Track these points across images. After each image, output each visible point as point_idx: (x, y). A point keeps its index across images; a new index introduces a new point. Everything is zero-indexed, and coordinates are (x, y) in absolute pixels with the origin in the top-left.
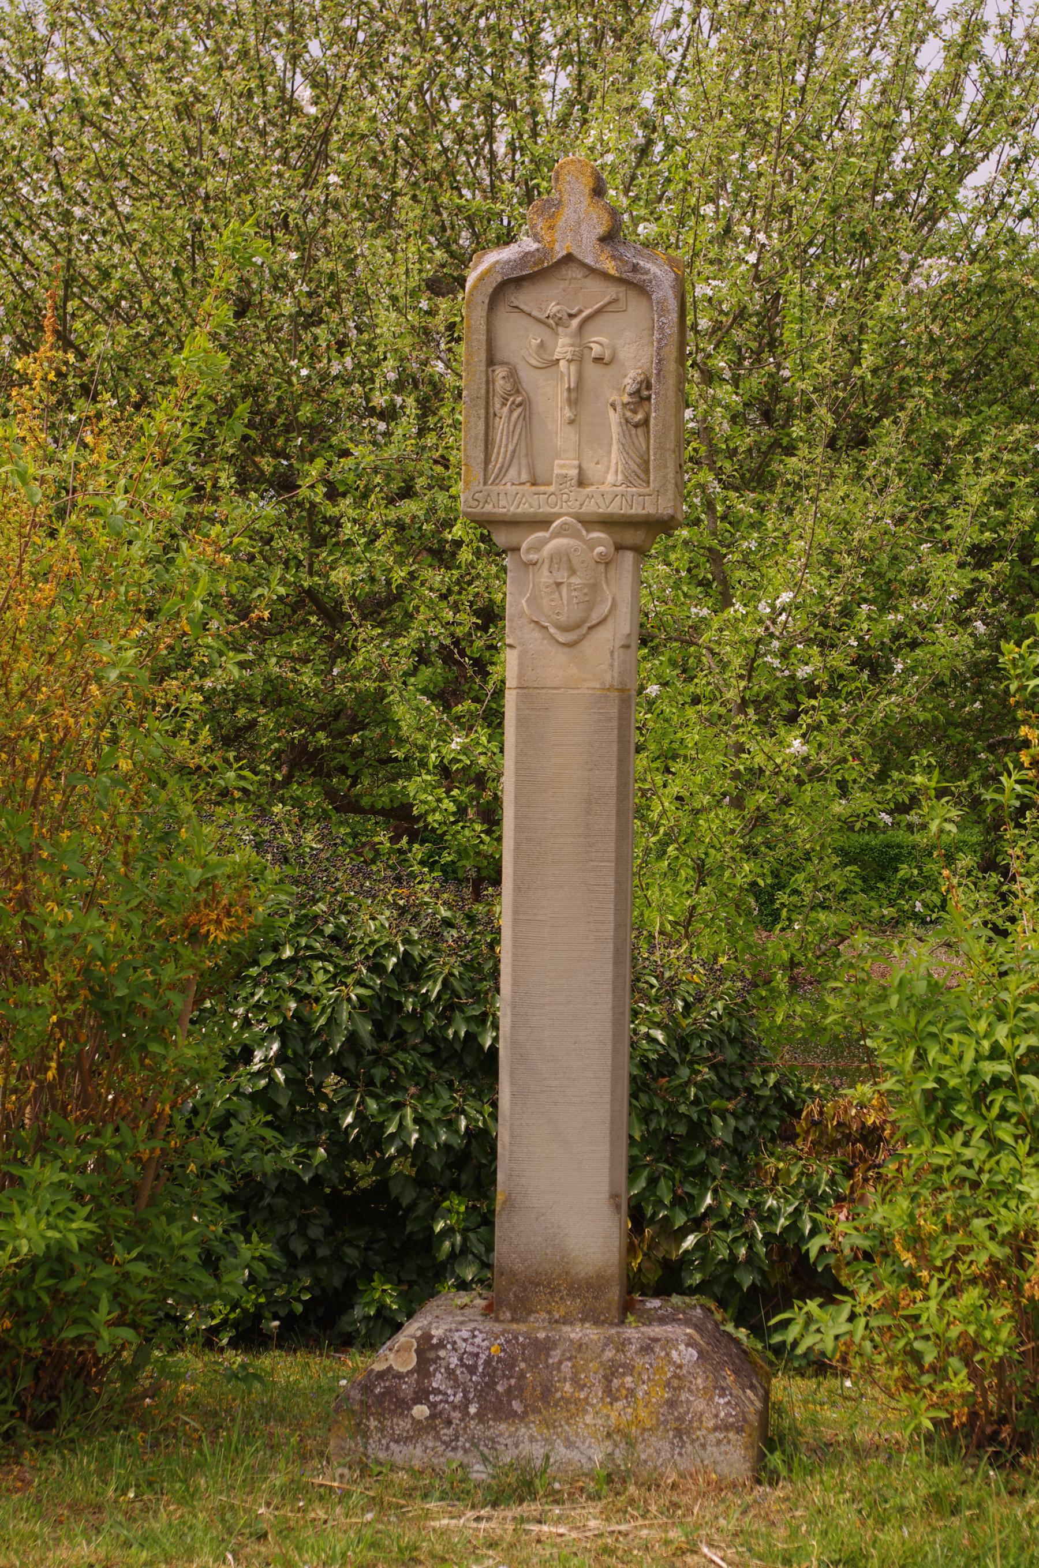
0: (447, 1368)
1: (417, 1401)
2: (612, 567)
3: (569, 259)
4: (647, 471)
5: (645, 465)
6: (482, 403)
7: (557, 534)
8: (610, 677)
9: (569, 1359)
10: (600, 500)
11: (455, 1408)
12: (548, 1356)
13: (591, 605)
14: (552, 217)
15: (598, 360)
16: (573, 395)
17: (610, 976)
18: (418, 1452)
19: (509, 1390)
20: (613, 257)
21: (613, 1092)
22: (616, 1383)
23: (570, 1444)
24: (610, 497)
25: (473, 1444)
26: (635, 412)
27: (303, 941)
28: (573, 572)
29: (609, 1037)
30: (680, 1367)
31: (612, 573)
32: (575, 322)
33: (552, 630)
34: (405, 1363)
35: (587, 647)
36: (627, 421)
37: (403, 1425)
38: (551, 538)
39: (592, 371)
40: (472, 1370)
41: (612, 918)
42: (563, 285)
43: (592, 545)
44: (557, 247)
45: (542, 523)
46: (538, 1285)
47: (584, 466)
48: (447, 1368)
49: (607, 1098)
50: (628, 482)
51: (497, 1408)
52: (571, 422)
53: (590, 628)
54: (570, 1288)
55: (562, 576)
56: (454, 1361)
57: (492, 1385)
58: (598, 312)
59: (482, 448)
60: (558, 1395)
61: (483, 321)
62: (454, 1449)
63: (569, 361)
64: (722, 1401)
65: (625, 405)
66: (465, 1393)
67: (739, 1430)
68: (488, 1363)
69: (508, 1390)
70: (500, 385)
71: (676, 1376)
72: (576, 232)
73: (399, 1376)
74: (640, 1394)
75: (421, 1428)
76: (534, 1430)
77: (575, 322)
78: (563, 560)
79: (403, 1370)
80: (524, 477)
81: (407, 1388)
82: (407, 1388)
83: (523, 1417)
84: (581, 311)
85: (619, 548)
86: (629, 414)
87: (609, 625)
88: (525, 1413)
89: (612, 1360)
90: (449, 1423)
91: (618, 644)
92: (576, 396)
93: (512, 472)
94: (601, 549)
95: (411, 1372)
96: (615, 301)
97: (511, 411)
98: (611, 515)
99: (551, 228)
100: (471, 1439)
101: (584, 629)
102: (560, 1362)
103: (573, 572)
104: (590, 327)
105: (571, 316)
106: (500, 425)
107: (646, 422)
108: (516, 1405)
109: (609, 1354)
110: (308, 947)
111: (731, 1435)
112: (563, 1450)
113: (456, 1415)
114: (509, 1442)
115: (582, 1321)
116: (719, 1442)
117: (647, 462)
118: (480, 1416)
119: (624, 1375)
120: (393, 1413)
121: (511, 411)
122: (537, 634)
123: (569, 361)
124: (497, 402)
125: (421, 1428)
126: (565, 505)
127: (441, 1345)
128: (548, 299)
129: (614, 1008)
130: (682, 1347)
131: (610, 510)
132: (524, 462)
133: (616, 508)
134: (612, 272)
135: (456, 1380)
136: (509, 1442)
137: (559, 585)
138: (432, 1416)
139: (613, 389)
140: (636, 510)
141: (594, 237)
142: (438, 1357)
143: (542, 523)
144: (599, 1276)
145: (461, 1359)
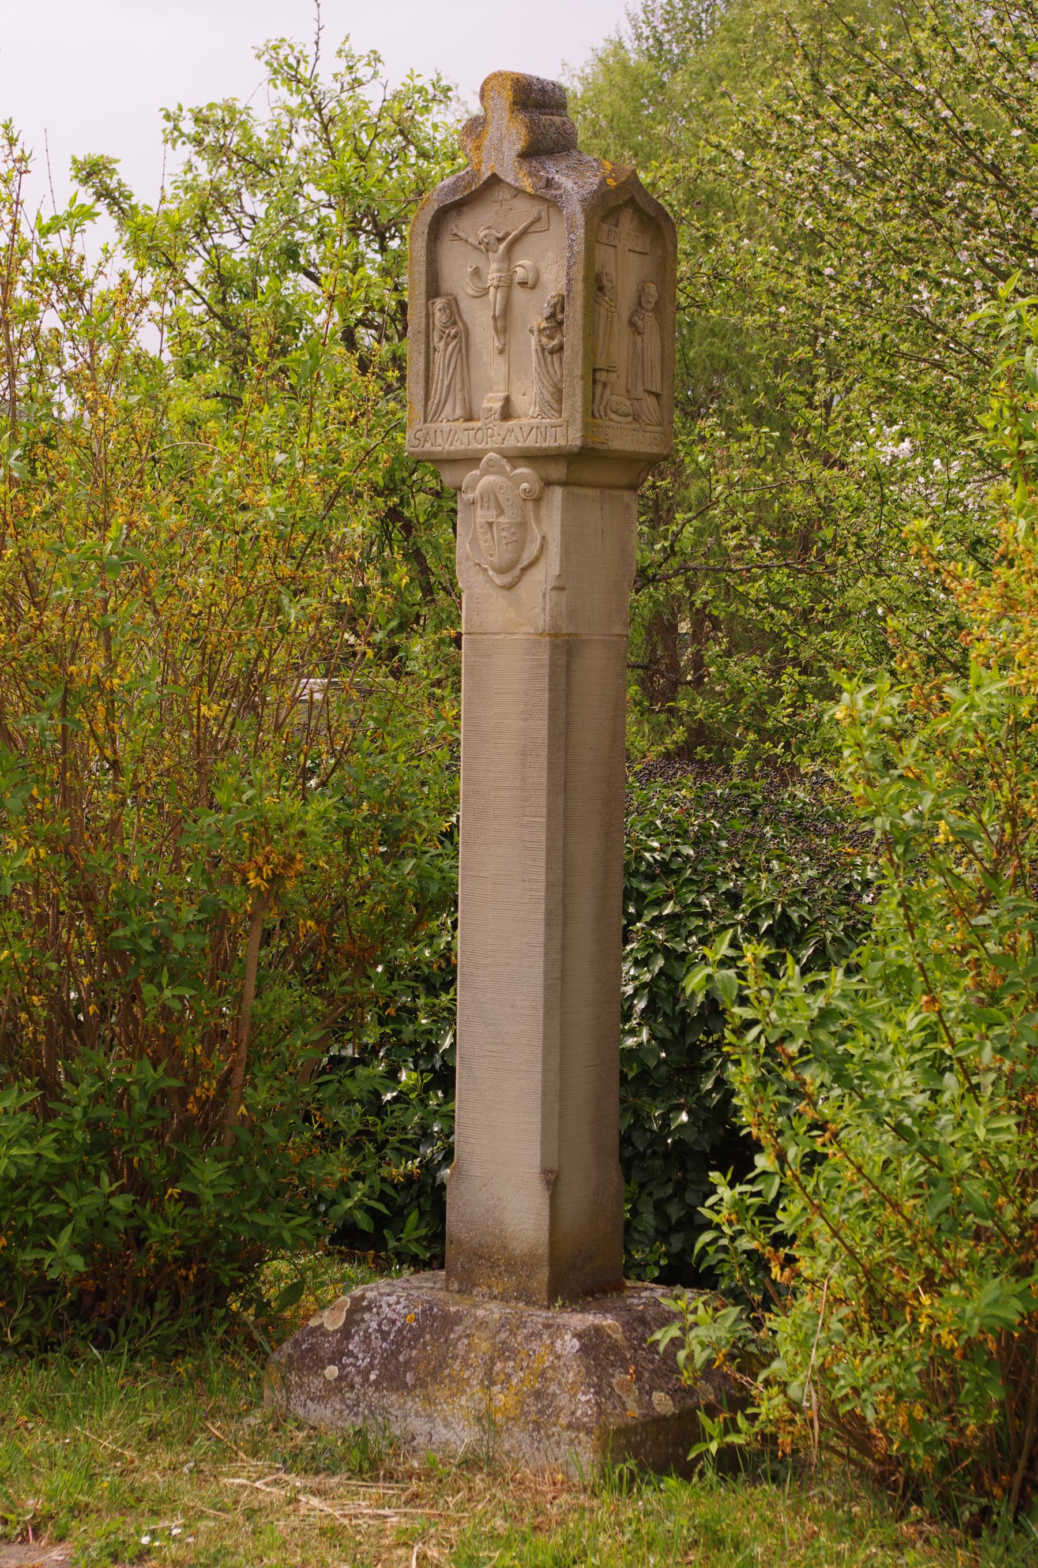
0: (366, 1331)
1: (332, 1362)
2: (544, 504)
3: (494, 180)
4: (560, 401)
5: (558, 395)
6: (422, 337)
7: (486, 472)
8: (543, 621)
9: (468, 1336)
10: (519, 434)
11: (358, 1372)
12: (451, 1330)
13: (521, 545)
14: (478, 136)
15: (523, 284)
16: (500, 324)
17: (541, 939)
18: (328, 1413)
19: (407, 1362)
20: (530, 174)
21: (545, 1062)
22: (499, 1366)
23: (447, 1425)
24: (526, 430)
25: (372, 1412)
26: (551, 338)
27: (690, 898)
28: (501, 512)
29: (540, 1003)
30: (558, 1357)
31: (544, 511)
32: (502, 246)
33: (491, 573)
34: (334, 1322)
35: (522, 589)
36: (543, 349)
37: (316, 1384)
38: (482, 476)
39: (520, 295)
40: (385, 1336)
41: (543, 877)
42: (496, 207)
43: (517, 481)
44: (483, 169)
45: (472, 460)
46: (480, 1257)
47: (513, 398)
48: (366, 1331)
49: (539, 1067)
50: (542, 414)
51: (392, 1378)
52: (501, 352)
53: (524, 570)
54: (508, 1264)
55: (491, 515)
56: (374, 1325)
57: (395, 1354)
58: (524, 233)
59: (422, 384)
60: (446, 1372)
61: (423, 252)
62: (356, 1414)
63: (497, 288)
64: (584, 1398)
65: (541, 331)
66: (373, 1358)
67: (589, 1432)
68: (400, 1331)
69: (413, 1361)
70: (439, 318)
71: (552, 1367)
72: (499, 150)
73: (325, 1334)
74: (514, 1381)
75: (335, 1388)
76: (419, 1405)
77: (502, 246)
78: (491, 498)
79: (331, 1328)
80: (458, 412)
81: (328, 1346)
82: (328, 1346)
83: (409, 1390)
84: (508, 234)
85: (548, 483)
86: (544, 340)
87: (541, 566)
88: (414, 1386)
89: (503, 1342)
90: (352, 1387)
91: (551, 584)
92: (504, 322)
93: (448, 408)
94: (525, 485)
95: (336, 1331)
96: (539, 219)
97: (447, 345)
98: (528, 449)
99: (478, 148)
100: (369, 1406)
101: (517, 571)
102: (459, 1338)
103: (501, 512)
104: (519, 249)
105: (500, 240)
106: (438, 358)
107: (561, 348)
108: (409, 1378)
109: (503, 1335)
110: (696, 904)
111: (582, 1435)
112: (443, 1431)
113: (358, 1379)
114: (399, 1413)
115: (518, 1299)
116: (571, 1442)
117: (560, 391)
118: (377, 1383)
119: (508, 1359)
120: (310, 1369)
121: (447, 345)
122: (481, 577)
123: (497, 288)
124: (436, 335)
125: (335, 1388)
126: (491, 437)
127: (369, 1308)
128: (477, 225)
129: (546, 972)
130: (567, 1337)
131: (527, 444)
132: (459, 397)
133: (532, 442)
134: (529, 190)
135: (369, 1345)
136: (399, 1413)
137: (490, 524)
138: (340, 1378)
139: (532, 313)
140: (550, 443)
141: (514, 154)
142: (363, 1320)
143: (472, 460)
144: (532, 1255)
145: (380, 1325)
